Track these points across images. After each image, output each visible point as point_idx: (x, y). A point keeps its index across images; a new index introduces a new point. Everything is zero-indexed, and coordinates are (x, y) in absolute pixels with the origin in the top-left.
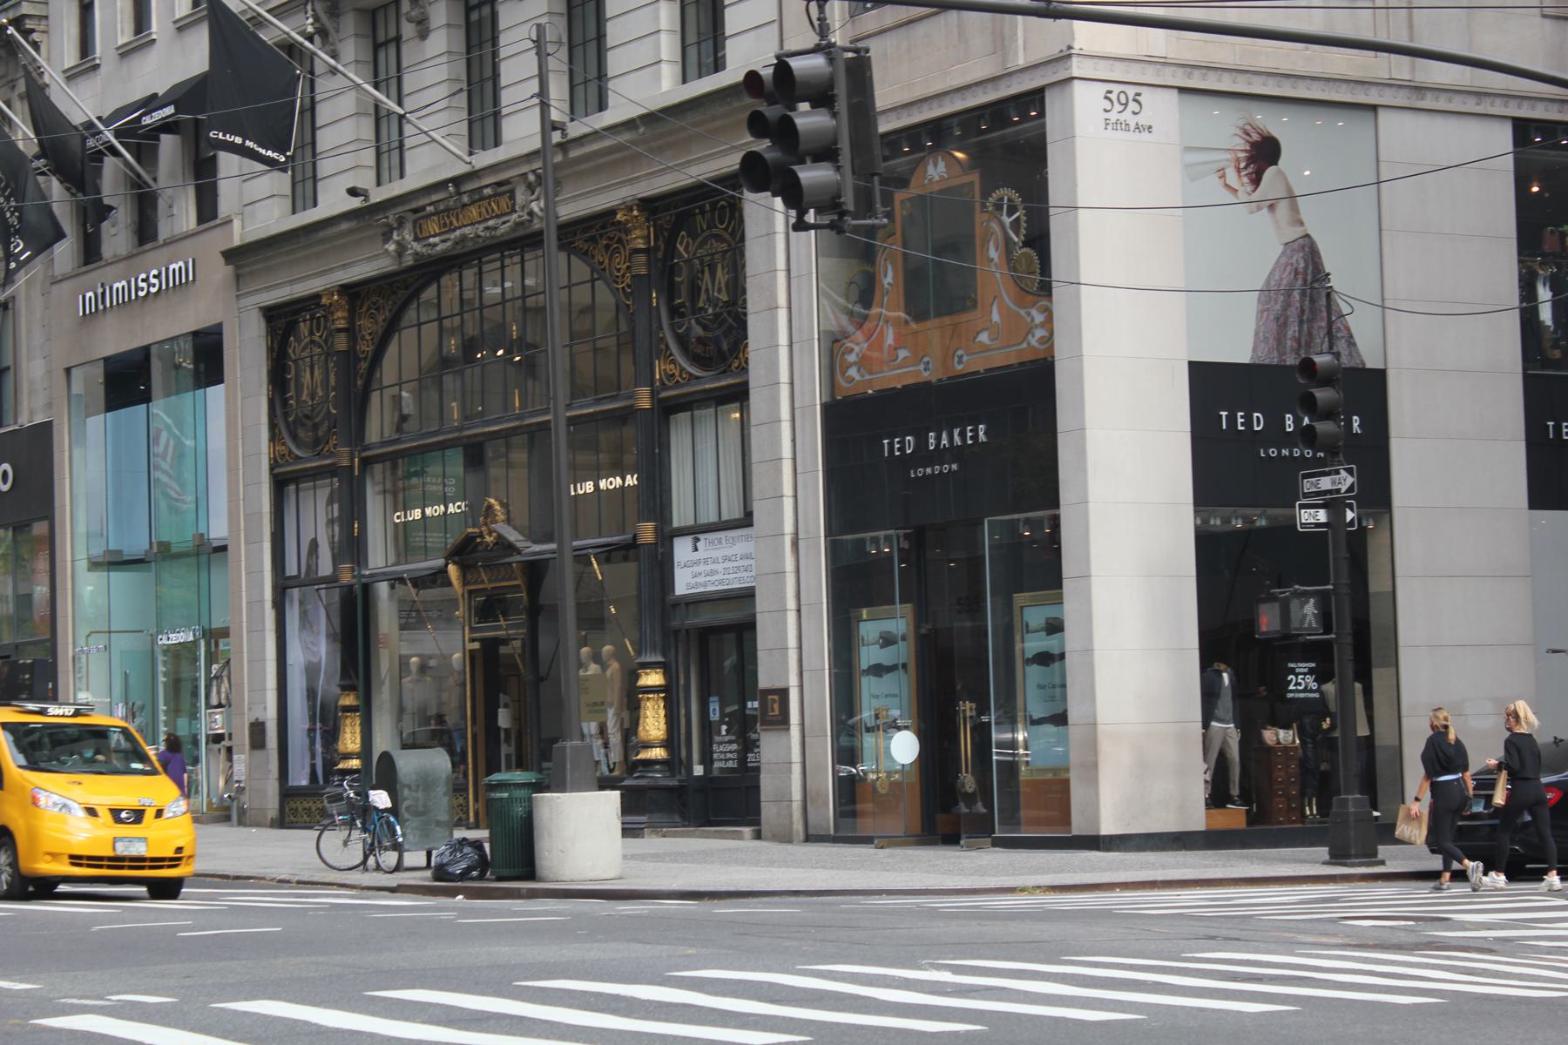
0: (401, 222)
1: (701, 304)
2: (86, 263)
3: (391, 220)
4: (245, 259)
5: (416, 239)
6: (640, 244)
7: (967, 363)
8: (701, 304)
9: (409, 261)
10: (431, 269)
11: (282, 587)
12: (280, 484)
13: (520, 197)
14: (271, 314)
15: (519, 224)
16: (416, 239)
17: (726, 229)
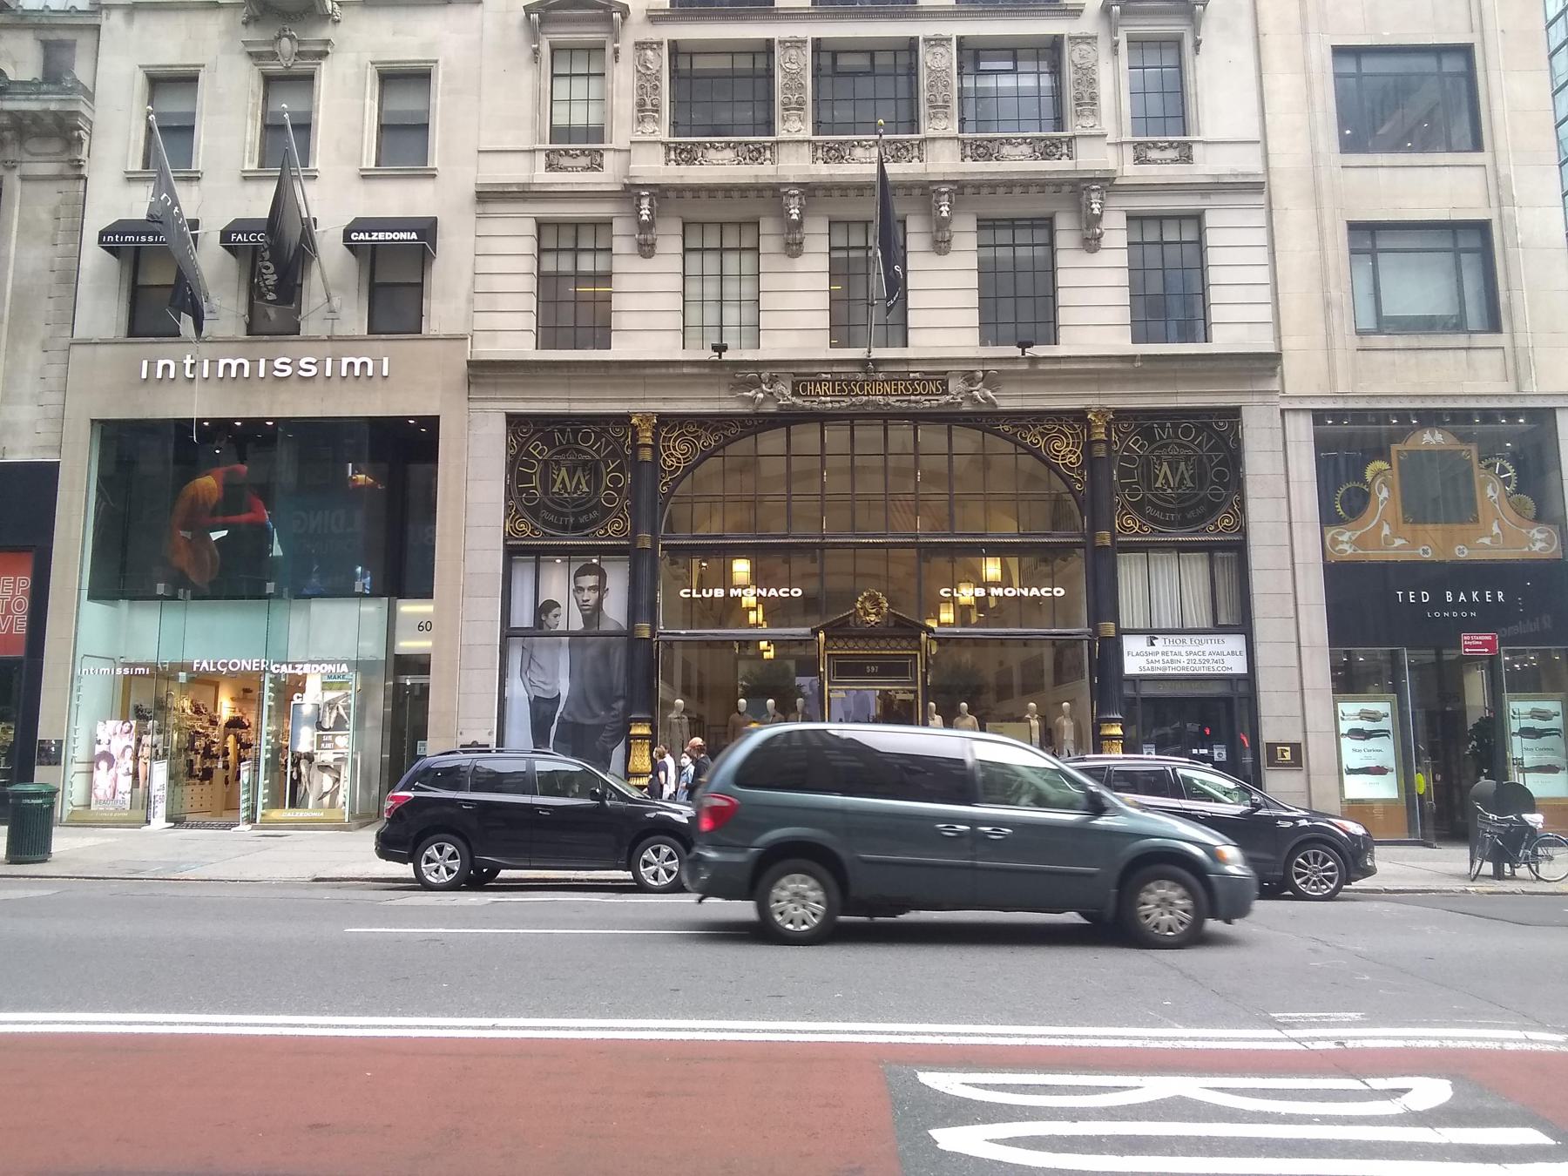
0: (773, 380)
1: (1158, 485)
2: (130, 335)
3: (765, 375)
4: (484, 374)
5: (795, 393)
6: (1103, 437)
7: (1462, 553)
8: (1158, 485)
9: (771, 408)
10: (787, 419)
11: (509, 633)
12: (512, 552)
13: (955, 385)
14: (513, 421)
15: (948, 403)
16: (795, 393)
17: (1192, 441)
